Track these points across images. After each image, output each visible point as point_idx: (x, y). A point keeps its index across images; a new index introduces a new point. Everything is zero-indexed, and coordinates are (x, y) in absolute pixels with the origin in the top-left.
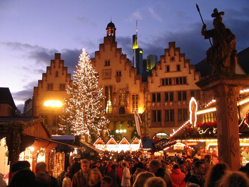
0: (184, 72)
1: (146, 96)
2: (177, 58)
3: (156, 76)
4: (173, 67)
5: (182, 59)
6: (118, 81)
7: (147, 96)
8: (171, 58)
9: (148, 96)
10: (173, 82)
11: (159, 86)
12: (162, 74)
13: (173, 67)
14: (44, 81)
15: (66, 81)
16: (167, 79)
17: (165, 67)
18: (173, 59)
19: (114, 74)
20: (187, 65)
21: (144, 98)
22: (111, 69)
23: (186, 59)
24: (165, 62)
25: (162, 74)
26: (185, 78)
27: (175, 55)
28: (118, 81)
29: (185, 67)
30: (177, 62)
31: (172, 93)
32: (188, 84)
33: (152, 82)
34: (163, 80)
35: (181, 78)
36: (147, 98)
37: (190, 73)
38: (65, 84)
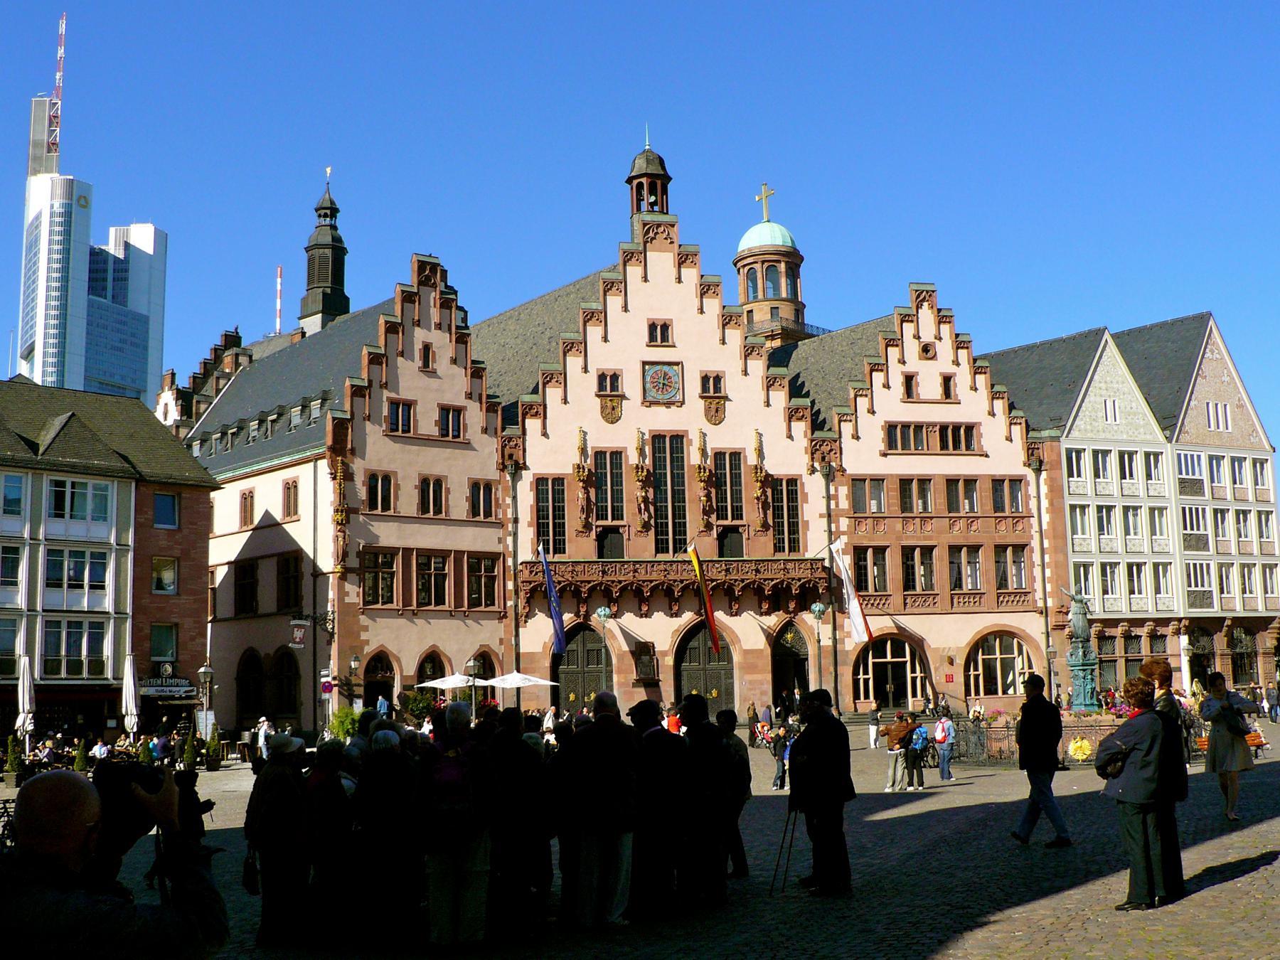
0: (973, 404)
2: (945, 349)
4: (929, 386)
7: (836, 490)
9: (840, 488)
13: (929, 386)
14: (375, 385)
15: (469, 396)
16: (906, 426)
17: (901, 379)
18: (927, 351)
19: (693, 387)
22: (677, 364)
23: (976, 353)
24: (902, 361)
25: (890, 404)
26: (970, 428)
30: (943, 363)
31: (924, 482)
32: (987, 456)
33: (856, 437)
34: (891, 428)
35: (956, 428)
36: (836, 497)
38: (464, 408)
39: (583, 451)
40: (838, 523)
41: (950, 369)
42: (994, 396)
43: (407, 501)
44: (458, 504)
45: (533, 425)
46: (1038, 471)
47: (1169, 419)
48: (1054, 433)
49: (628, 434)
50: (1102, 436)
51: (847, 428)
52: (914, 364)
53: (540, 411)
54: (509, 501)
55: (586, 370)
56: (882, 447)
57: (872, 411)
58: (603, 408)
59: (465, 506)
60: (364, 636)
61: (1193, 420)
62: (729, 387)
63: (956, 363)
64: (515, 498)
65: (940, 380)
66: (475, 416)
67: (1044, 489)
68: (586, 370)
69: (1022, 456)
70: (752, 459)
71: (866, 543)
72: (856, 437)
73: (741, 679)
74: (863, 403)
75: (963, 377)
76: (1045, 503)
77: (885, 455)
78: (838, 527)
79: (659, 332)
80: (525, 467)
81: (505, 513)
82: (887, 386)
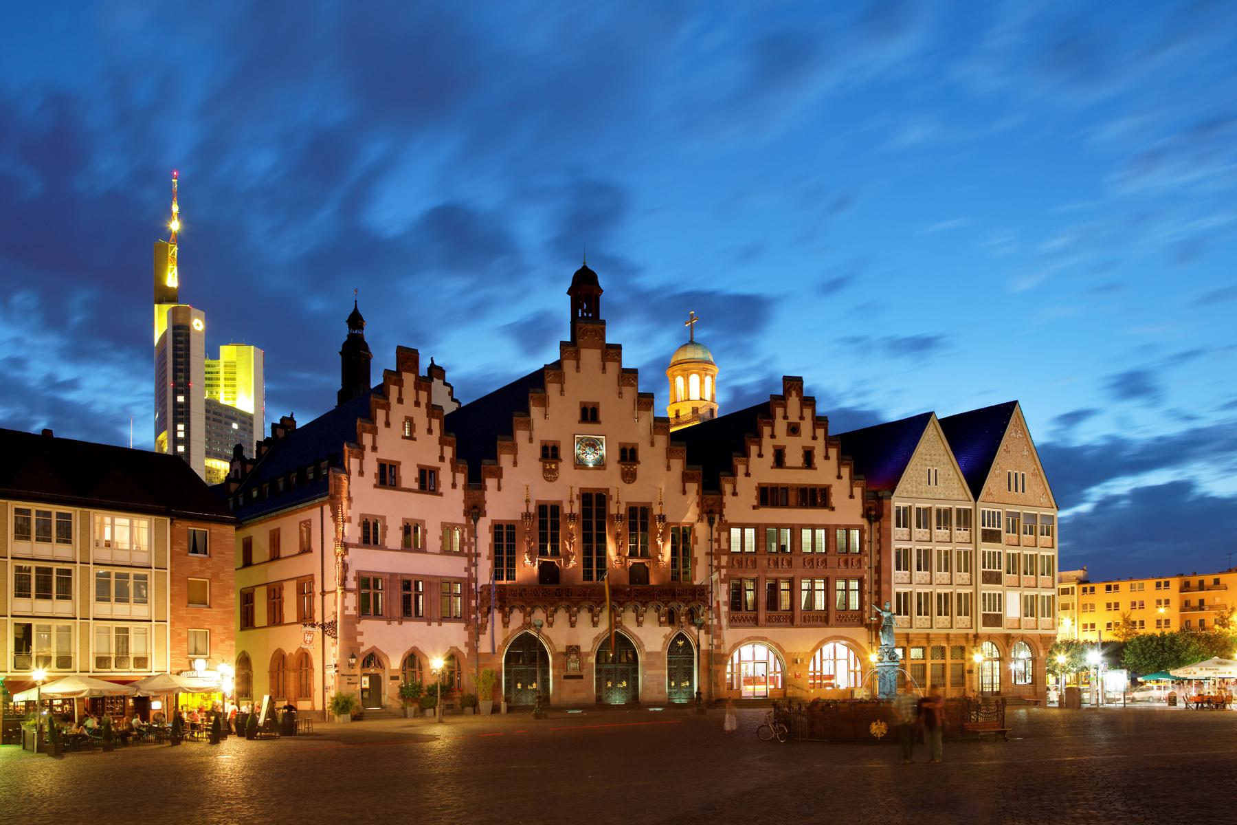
0: (827, 470)
1: (715, 535)
2: (806, 427)
3: (747, 475)
4: (794, 457)
5: (820, 433)
6: (629, 476)
8: (789, 424)
10: (792, 499)
11: (754, 508)
12: (759, 469)
13: (794, 457)
15: (442, 459)
17: (772, 451)
20: (833, 452)
21: (711, 540)
23: (832, 433)
24: (773, 436)
27: (802, 418)
28: (629, 476)
29: (827, 457)
30: (805, 439)
33: (735, 494)
36: (718, 540)
37: (839, 477)
38: (439, 469)
39: (527, 501)
40: (718, 559)
41: (810, 443)
42: (840, 464)
43: (394, 537)
44: (434, 542)
45: (491, 483)
46: (870, 522)
47: (975, 480)
48: (886, 493)
49: (564, 490)
50: (924, 495)
51: (728, 488)
52: (782, 438)
53: (498, 474)
54: (473, 540)
55: (531, 440)
56: (755, 503)
57: (747, 475)
58: (545, 471)
59: (439, 543)
60: (359, 639)
61: (994, 482)
62: (641, 455)
63: (814, 438)
64: (476, 538)
65: (802, 452)
66: (445, 476)
67: (875, 536)
68: (531, 440)
69: (860, 510)
70: (656, 511)
71: (740, 575)
72: (735, 494)
73: (644, 674)
74: (741, 469)
75: (819, 447)
76: (875, 546)
77: (754, 508)
78: (719, 562)
79: (590, 414)
80: (485, 515)
81: (470, 549)
82: (760, 455)
